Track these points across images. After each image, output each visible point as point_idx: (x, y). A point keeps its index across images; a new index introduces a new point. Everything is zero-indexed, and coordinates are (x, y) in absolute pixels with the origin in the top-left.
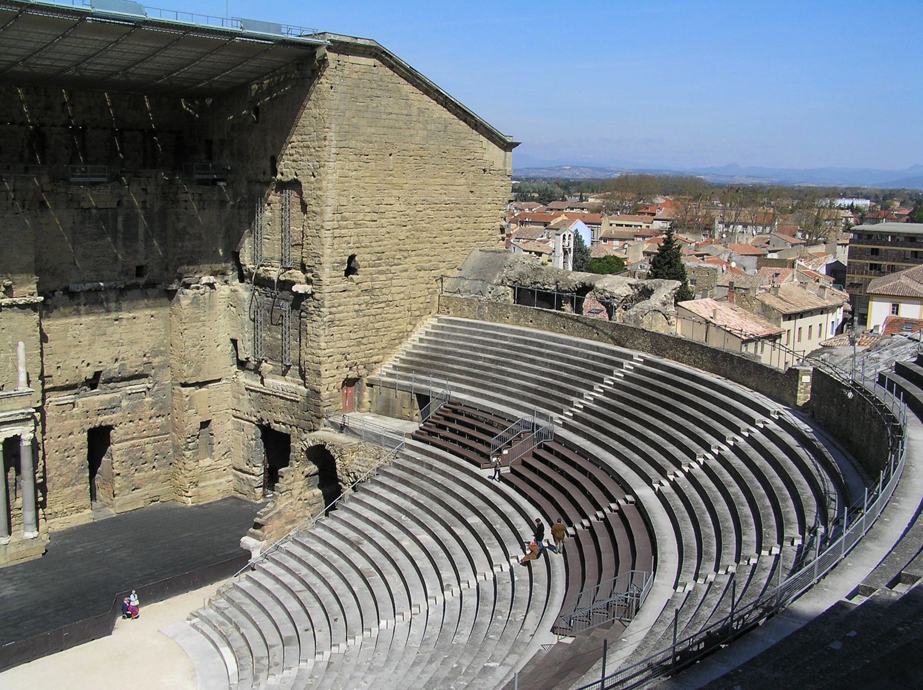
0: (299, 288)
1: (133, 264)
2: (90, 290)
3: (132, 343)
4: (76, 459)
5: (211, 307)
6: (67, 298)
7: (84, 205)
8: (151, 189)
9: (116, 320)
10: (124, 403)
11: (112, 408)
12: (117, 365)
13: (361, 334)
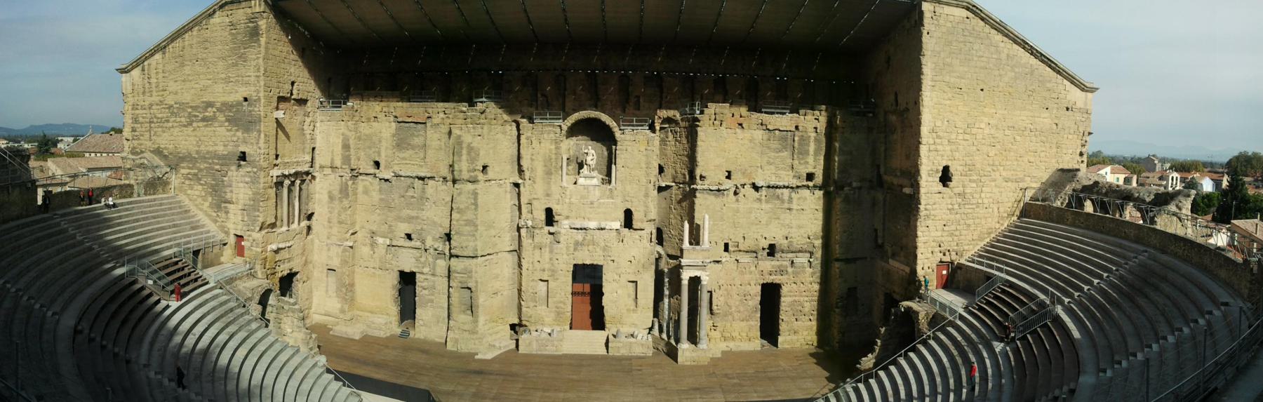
0: (907, 190)
1: (804, 171)
3: (799, 227)
4: (750, 303)
7: (770, 127)
10: (790, 270)
11: (782, 272)
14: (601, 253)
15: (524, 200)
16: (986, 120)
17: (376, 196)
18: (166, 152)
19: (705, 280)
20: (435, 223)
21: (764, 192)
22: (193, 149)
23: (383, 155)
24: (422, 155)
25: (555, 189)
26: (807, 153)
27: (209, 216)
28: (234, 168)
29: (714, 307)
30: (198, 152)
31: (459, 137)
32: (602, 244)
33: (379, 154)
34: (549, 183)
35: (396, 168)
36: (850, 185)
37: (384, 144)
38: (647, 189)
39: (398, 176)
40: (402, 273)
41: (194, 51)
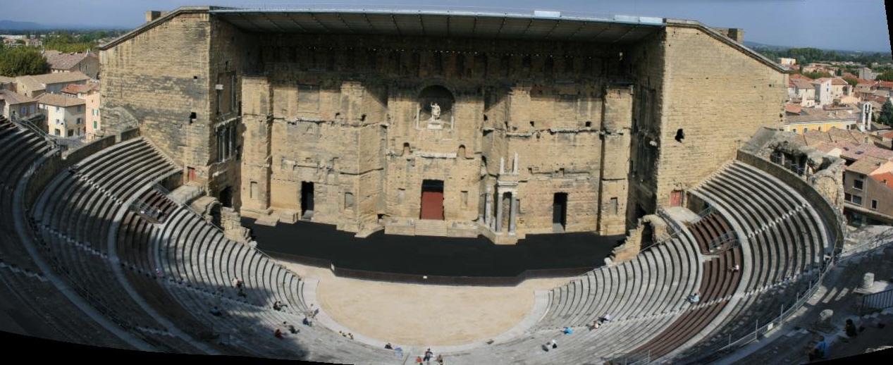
1: (584, 121)
2: (560, 132)
3: (581, 157)
5: (621, 144)
6: (549, 134)
7: (561, 93)
8: (596, 87)
9: (574, 146)
12: (572, 167)
13: (684, 169)
14: (443, 173)
15: (390, 137)
16: (710, 98)
17: (285, 134)
18: (134, 108)
19: (515, 193)
20: (326, 152)
21: (557, 135)
22: (155, 108)
23: (290, 106)
24: (317, 107)
25: (411, 131)
26: (587, 109)
27: (168, 154)
28: (187, 123)
29: (521, 210)
30: (159, 110)
31: (347, 97)
32: (444, 167)
33: (287, 105)
34: (407, 127)
35: (300, 115)
36: (615, 131)
37: (290, 99)
38: (476, 132)
39: (301, 121)
40: (304, 184)
41: (157, 41)
